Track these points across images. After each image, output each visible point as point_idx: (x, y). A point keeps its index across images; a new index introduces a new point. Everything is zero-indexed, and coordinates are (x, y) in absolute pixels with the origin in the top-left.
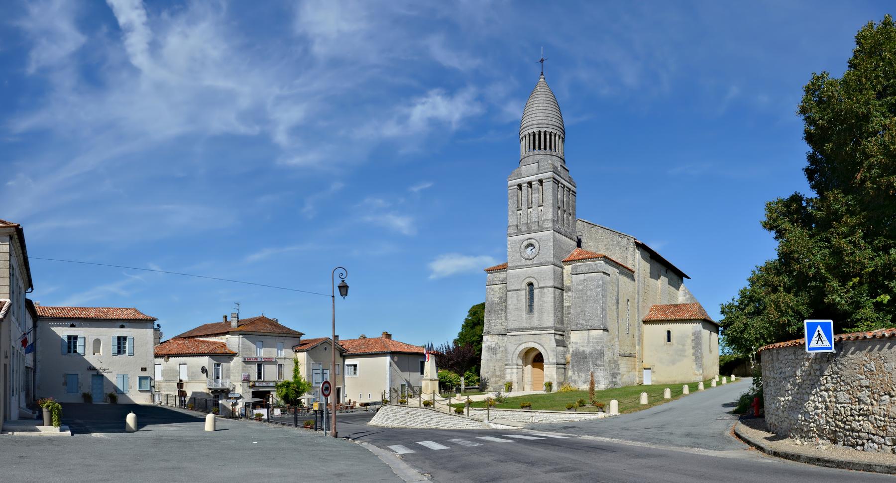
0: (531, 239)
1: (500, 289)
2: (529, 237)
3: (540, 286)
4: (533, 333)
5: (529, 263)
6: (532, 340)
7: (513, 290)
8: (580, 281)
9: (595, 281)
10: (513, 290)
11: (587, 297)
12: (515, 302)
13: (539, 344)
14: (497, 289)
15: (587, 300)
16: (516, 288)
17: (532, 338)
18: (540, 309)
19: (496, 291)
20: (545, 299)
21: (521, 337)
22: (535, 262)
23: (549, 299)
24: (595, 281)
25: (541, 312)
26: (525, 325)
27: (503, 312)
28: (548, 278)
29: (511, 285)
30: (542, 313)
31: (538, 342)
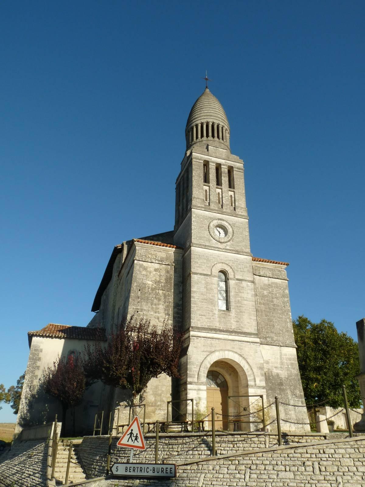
0: (223, 220)
1: (156, 270)
2: (220, 218)
3: (237, 277)
4: (231, 337)
5: (219, 245)
6: (229, 348)
7: (201, 274)
8: (265, 285)
9: (280, 289)
10: (201, 274)
11: (274, 305)
12: (203, 290)
13: (241, 355)
14: (152, 269)
15: (274, 310)
16: (205, 273)
17: (229, 346)
18: (237, 306)
19: (150, 272)
20: (245, 295)
21: (213, 341)
22: (228, 248)
23: (250, 296)
24: (280, 289)
25: (240, 312)
26: (217, 325)
27: (161, 303)
28: (246, 270)
29: (197, 267)
30: (241, 312)
31: (239, 351)
